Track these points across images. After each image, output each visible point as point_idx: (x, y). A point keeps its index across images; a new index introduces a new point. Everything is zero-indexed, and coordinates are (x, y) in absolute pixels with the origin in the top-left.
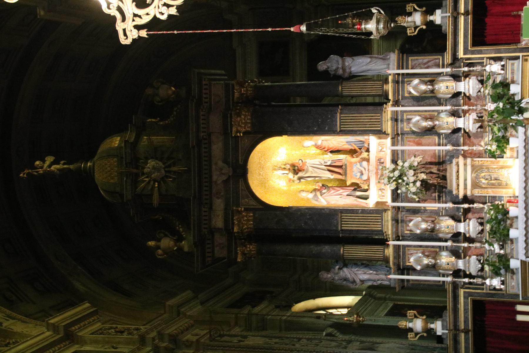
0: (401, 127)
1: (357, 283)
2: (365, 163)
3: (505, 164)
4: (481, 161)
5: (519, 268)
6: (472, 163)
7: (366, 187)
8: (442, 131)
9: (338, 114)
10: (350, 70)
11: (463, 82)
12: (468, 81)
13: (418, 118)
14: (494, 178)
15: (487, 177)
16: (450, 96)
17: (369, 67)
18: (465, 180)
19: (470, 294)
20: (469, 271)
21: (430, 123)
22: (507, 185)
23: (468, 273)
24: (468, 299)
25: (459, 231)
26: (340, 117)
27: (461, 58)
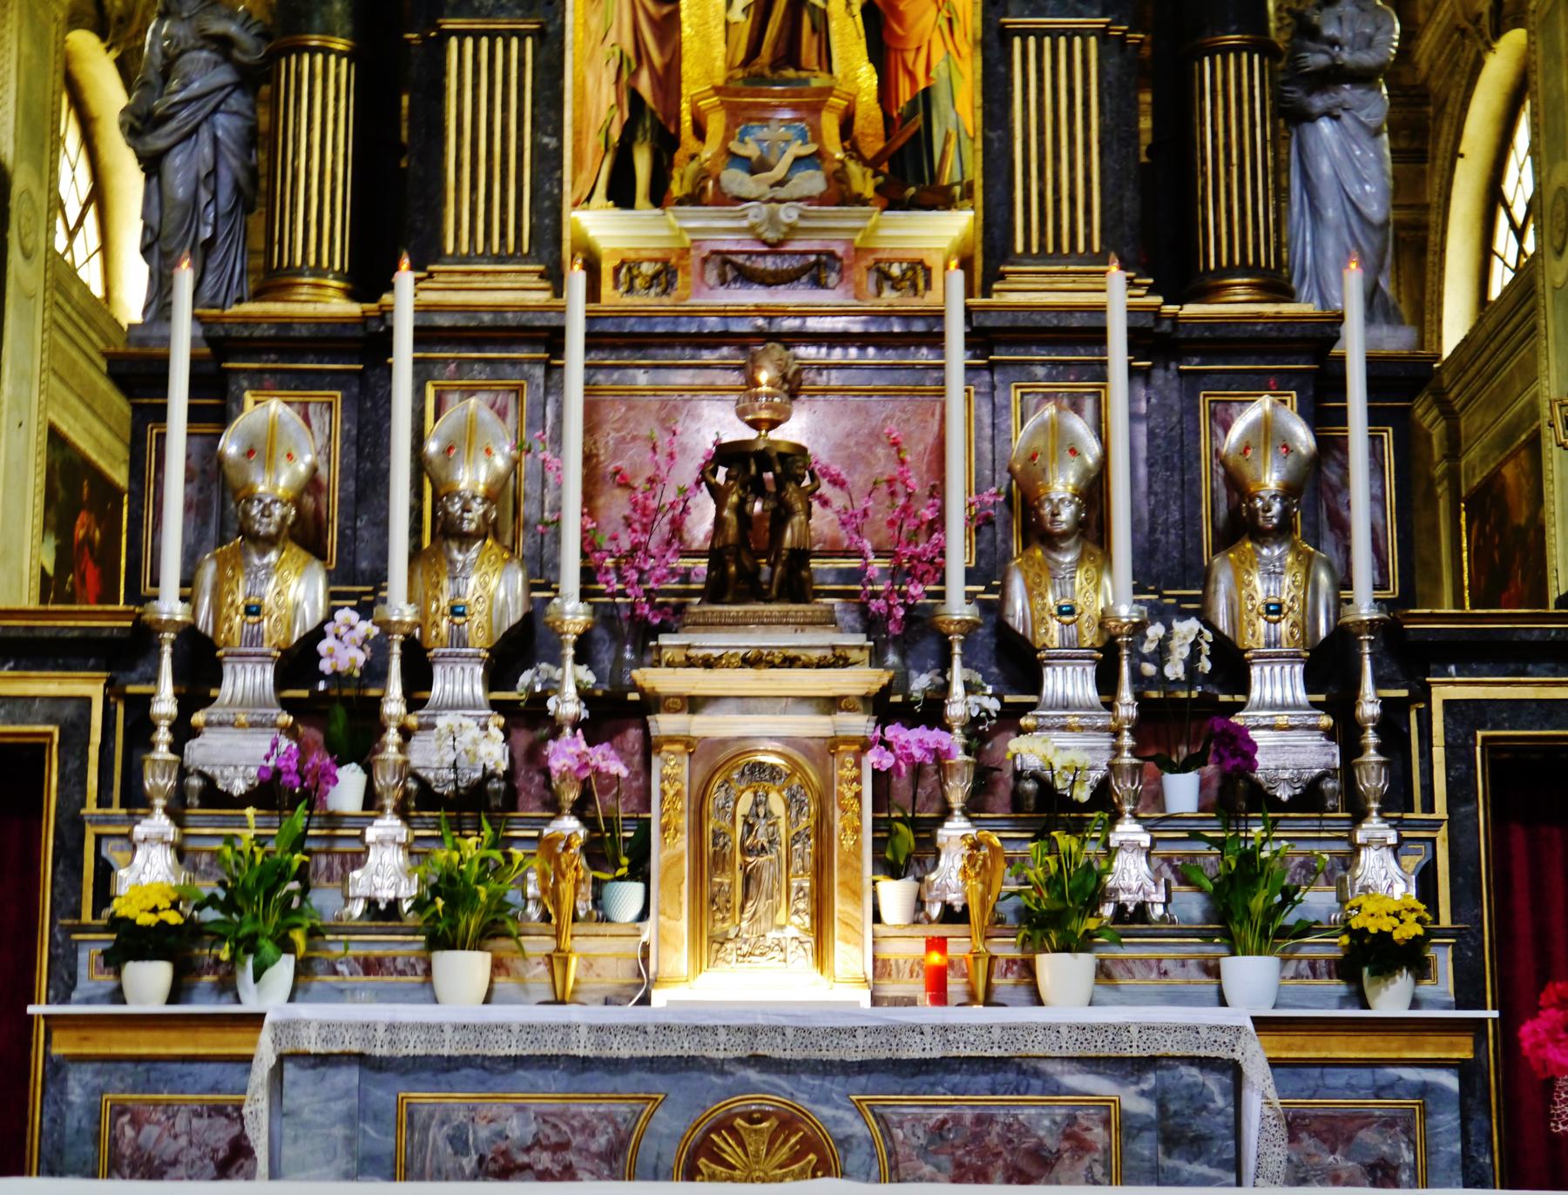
0: (1032, 363)
1: (149, 139)
2: (813, 182)
3: (838, 929)
4: (858, 795)
5: (238, 1001)
6: (848, 741)
7: (676, 189)
8: (1017, 587)
9: (1101, 21)
10: (1322, 115)
11: (1301, 696)
12: (1311, 721)
13: (1091, 450)
14: (758, 868)
15: (761, 827)
16: (1223, 623)
17: (1331, 213)
18: (745, 702)
19: (75, 733)
20: (208, 724)
21: (1066, 514)
22: (712, 940)
23: (198, 718)
24: (49, 720)
25: (438, 670)
26: (1084, 34)
27: (1427, 689)
